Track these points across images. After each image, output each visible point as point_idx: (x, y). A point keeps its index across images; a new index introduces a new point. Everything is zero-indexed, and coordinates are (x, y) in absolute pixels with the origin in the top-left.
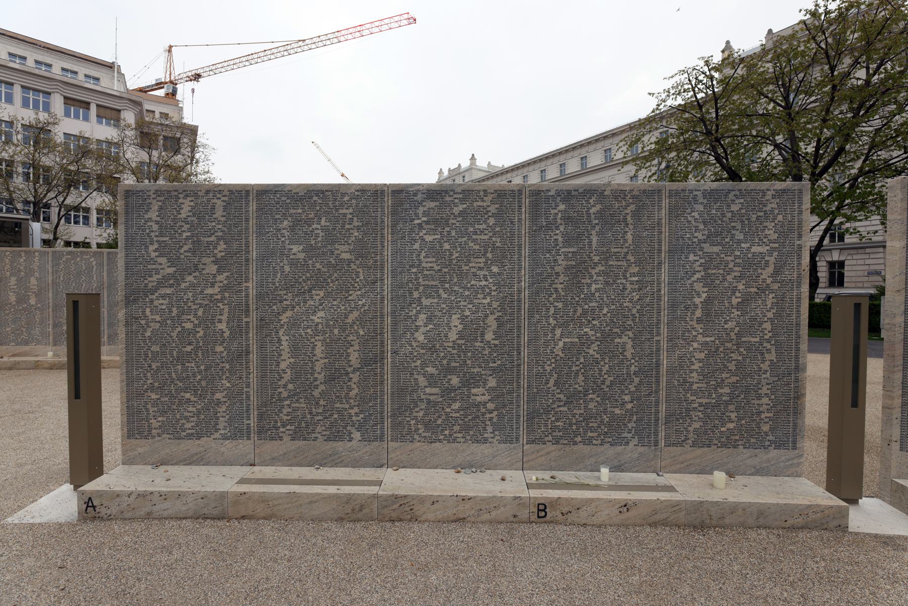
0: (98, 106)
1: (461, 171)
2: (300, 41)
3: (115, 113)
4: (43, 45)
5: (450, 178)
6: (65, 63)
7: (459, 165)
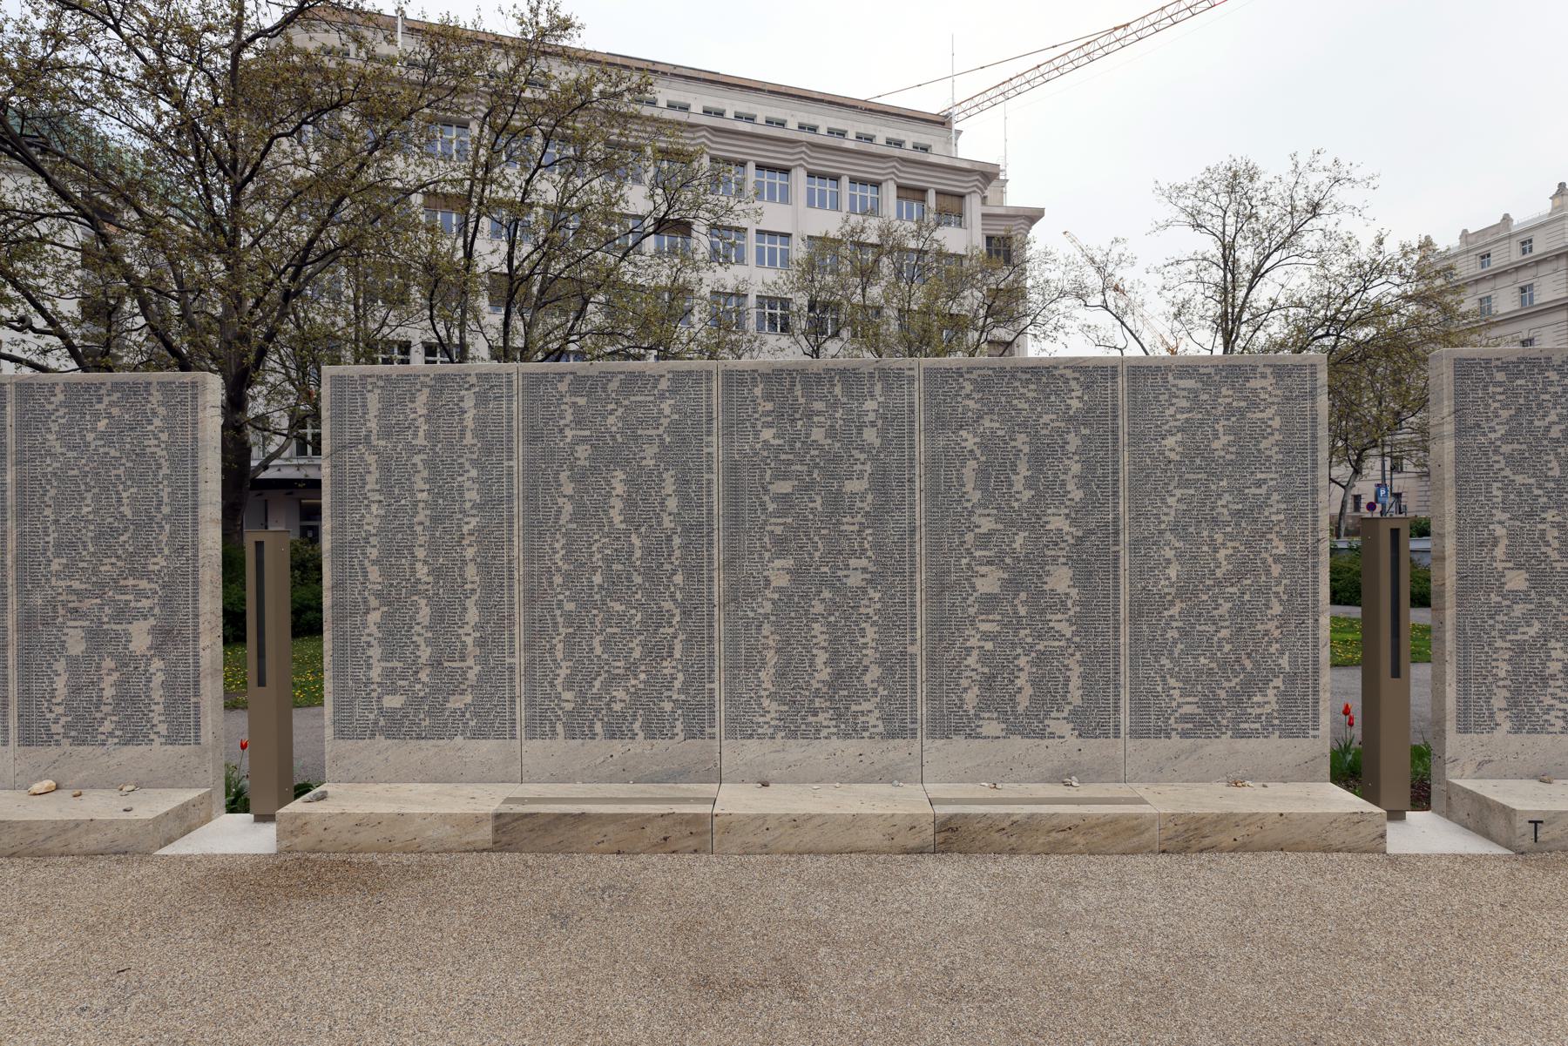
0: (938, 193)
1: (1513, 230)
2: (1116, 29)
3: (956, 200)
5: (1468, 251)
7: (1506, 218)
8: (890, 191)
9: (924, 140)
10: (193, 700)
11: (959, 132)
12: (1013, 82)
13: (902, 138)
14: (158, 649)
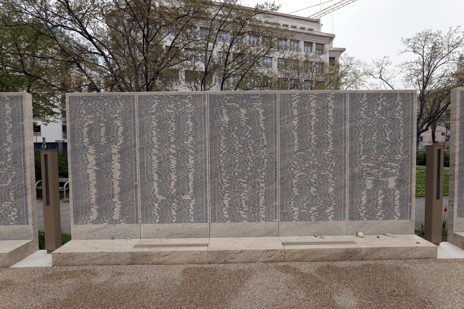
0: (316, 44)
3: (321, 46)
4: (294, 17)
6: (301, 24)
8: (302, 44)
9: (311, 27)
10: (409, 204)
11: (322, 25)
12: (327, 9)
13: (305, 27)
14: (398, 187)
